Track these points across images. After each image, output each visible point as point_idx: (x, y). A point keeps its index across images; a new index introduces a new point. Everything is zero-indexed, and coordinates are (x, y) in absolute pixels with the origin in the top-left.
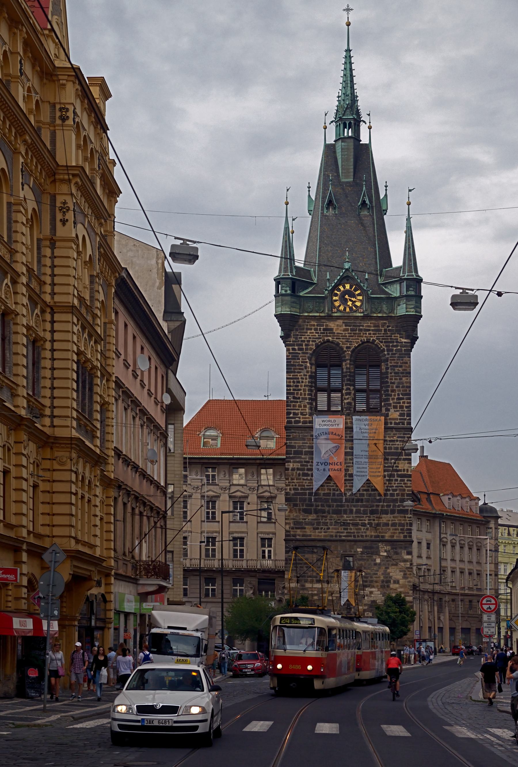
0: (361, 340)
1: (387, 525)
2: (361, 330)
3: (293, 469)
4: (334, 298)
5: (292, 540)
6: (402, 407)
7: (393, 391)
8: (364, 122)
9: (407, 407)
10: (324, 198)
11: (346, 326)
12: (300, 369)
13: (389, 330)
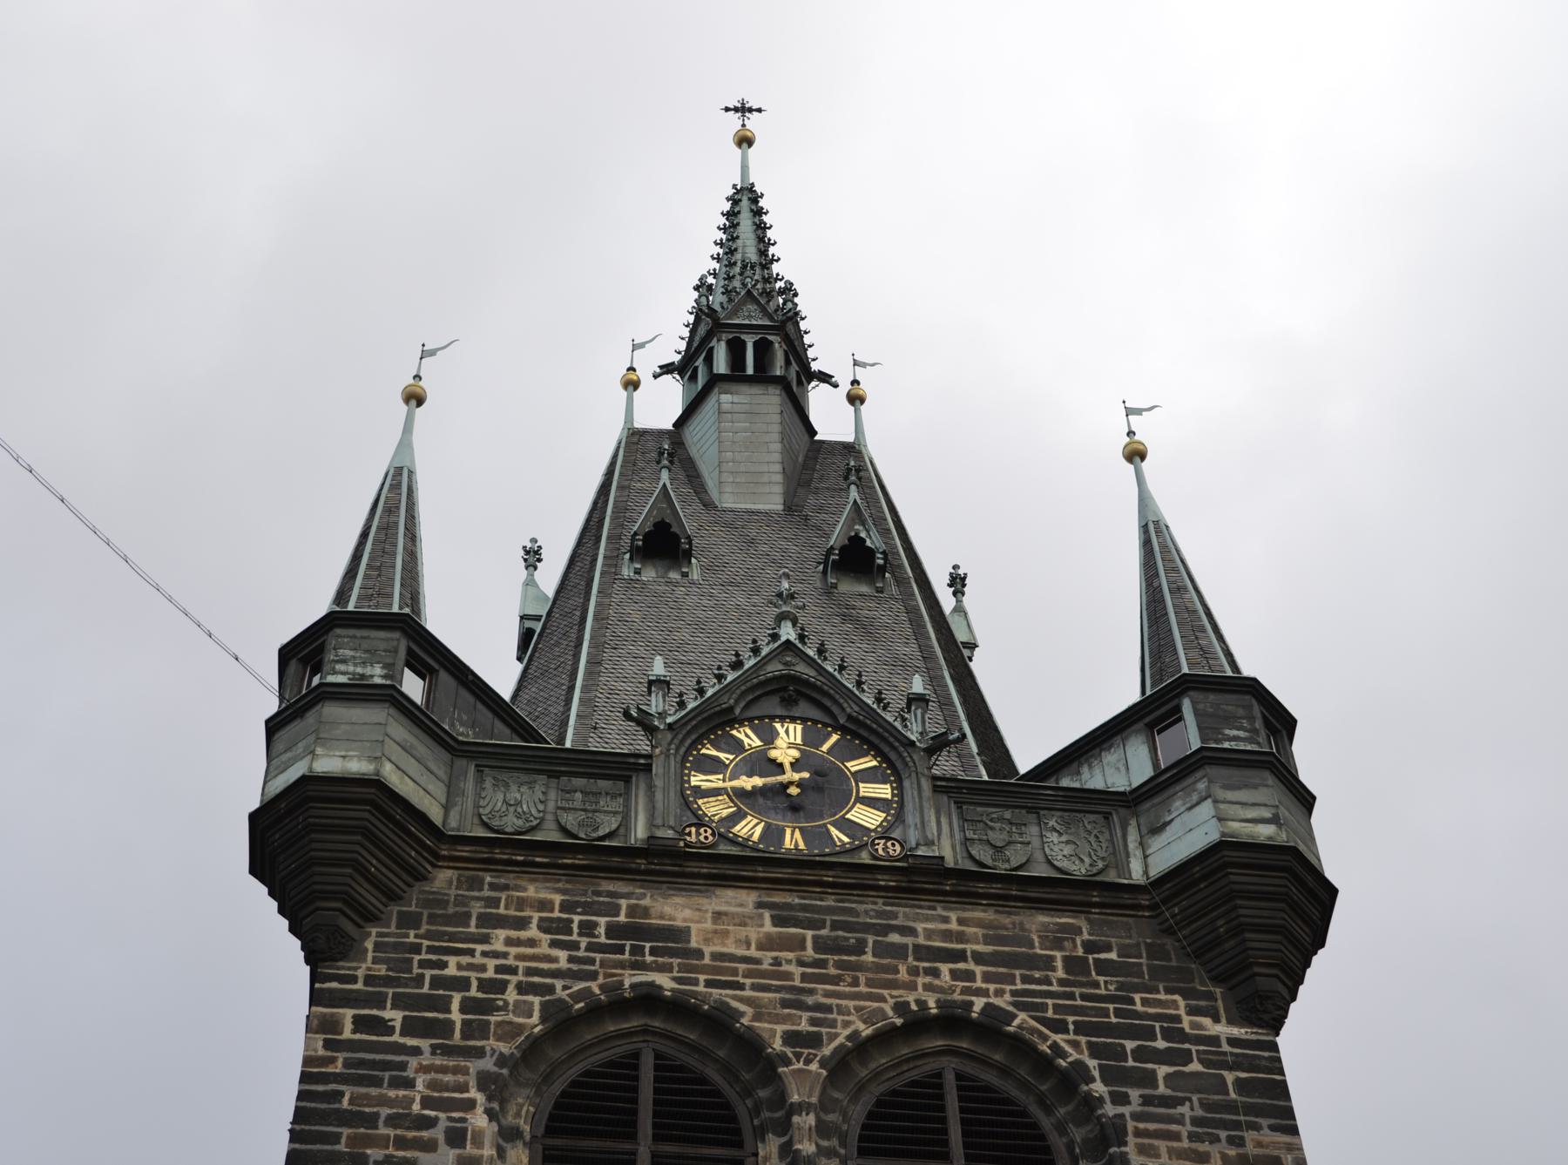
0: (901, 1008)
4: (696, 780)
8: (825, 378)
11: (778, 921)
12: (401, 1143)
13: (1104, 968)
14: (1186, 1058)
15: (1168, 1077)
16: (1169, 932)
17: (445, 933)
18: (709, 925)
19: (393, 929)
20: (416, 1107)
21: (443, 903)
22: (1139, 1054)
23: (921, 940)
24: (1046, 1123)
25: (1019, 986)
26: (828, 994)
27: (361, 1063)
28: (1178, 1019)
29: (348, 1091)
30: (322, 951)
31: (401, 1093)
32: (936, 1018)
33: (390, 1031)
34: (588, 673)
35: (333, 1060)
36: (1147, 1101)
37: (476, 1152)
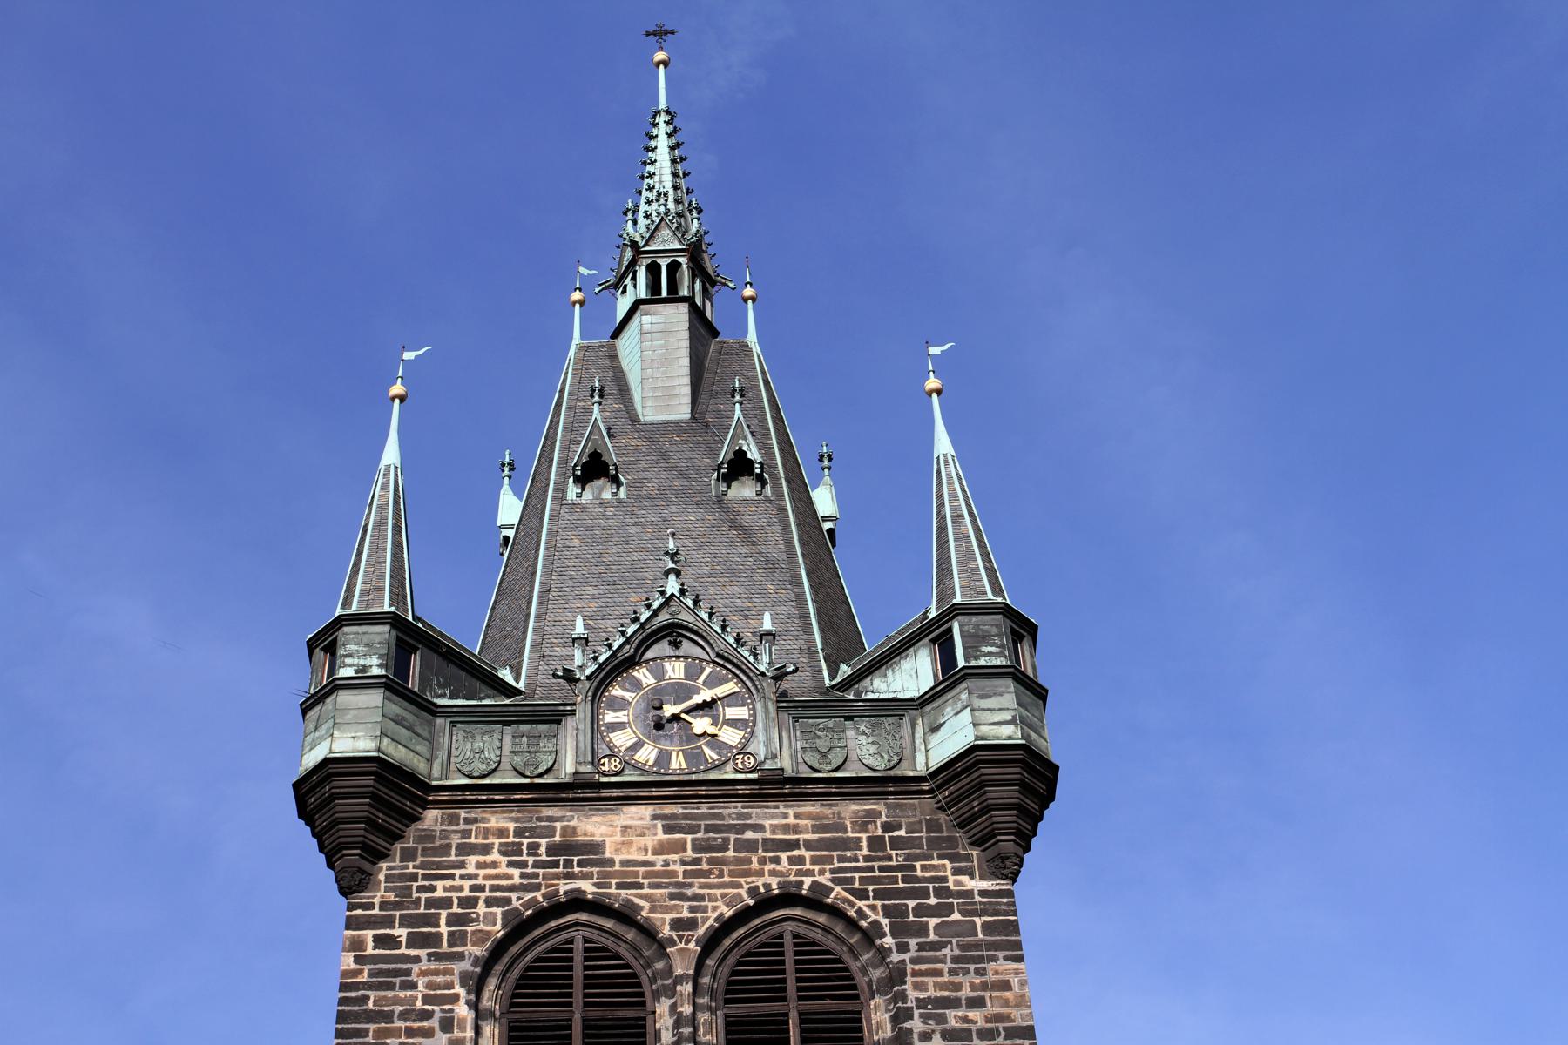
0: (753, 891)
2: (751, 846)
4: (609, 717)
11: (668, 829)
13: (896, 843)
14: (949, 909)
15: (937, 926)
16: (941, 808)
17: (434, 863)
18: (618, 838)
19: (398, 863)
20: (419, 1004)
21: (431, 838)
22: (919, 910)
23: (768, 835)
24: (854, 966)
25: (836, 865)
26: (702, 886)
27: (380, 973)
28: (945, 879)
29: (372, 995)
30: (352, 884)
31: (409, 993)
32: (777, 896)
33: (398, 945)
34: (540, 603)
35: (360, 972)
36: (921, 947)
37: (461, 1035)
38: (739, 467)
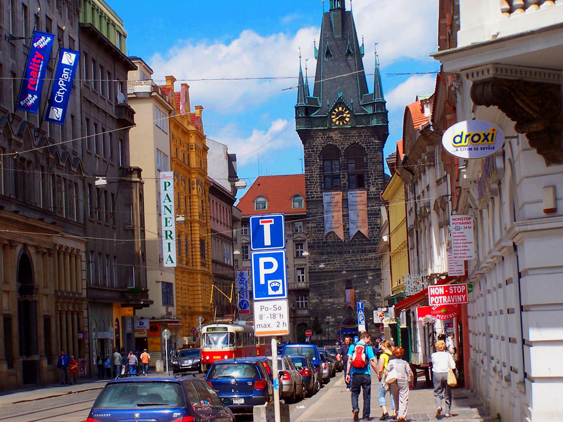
1: (371, 259)
2: (350, 136)
3: (311, 228)
4: (333, 117)
5: (313, 272)
6: (377, 184)
7: (372, 174)
9: (381, 184)
10: (324, 50)
38: (349, 52)
